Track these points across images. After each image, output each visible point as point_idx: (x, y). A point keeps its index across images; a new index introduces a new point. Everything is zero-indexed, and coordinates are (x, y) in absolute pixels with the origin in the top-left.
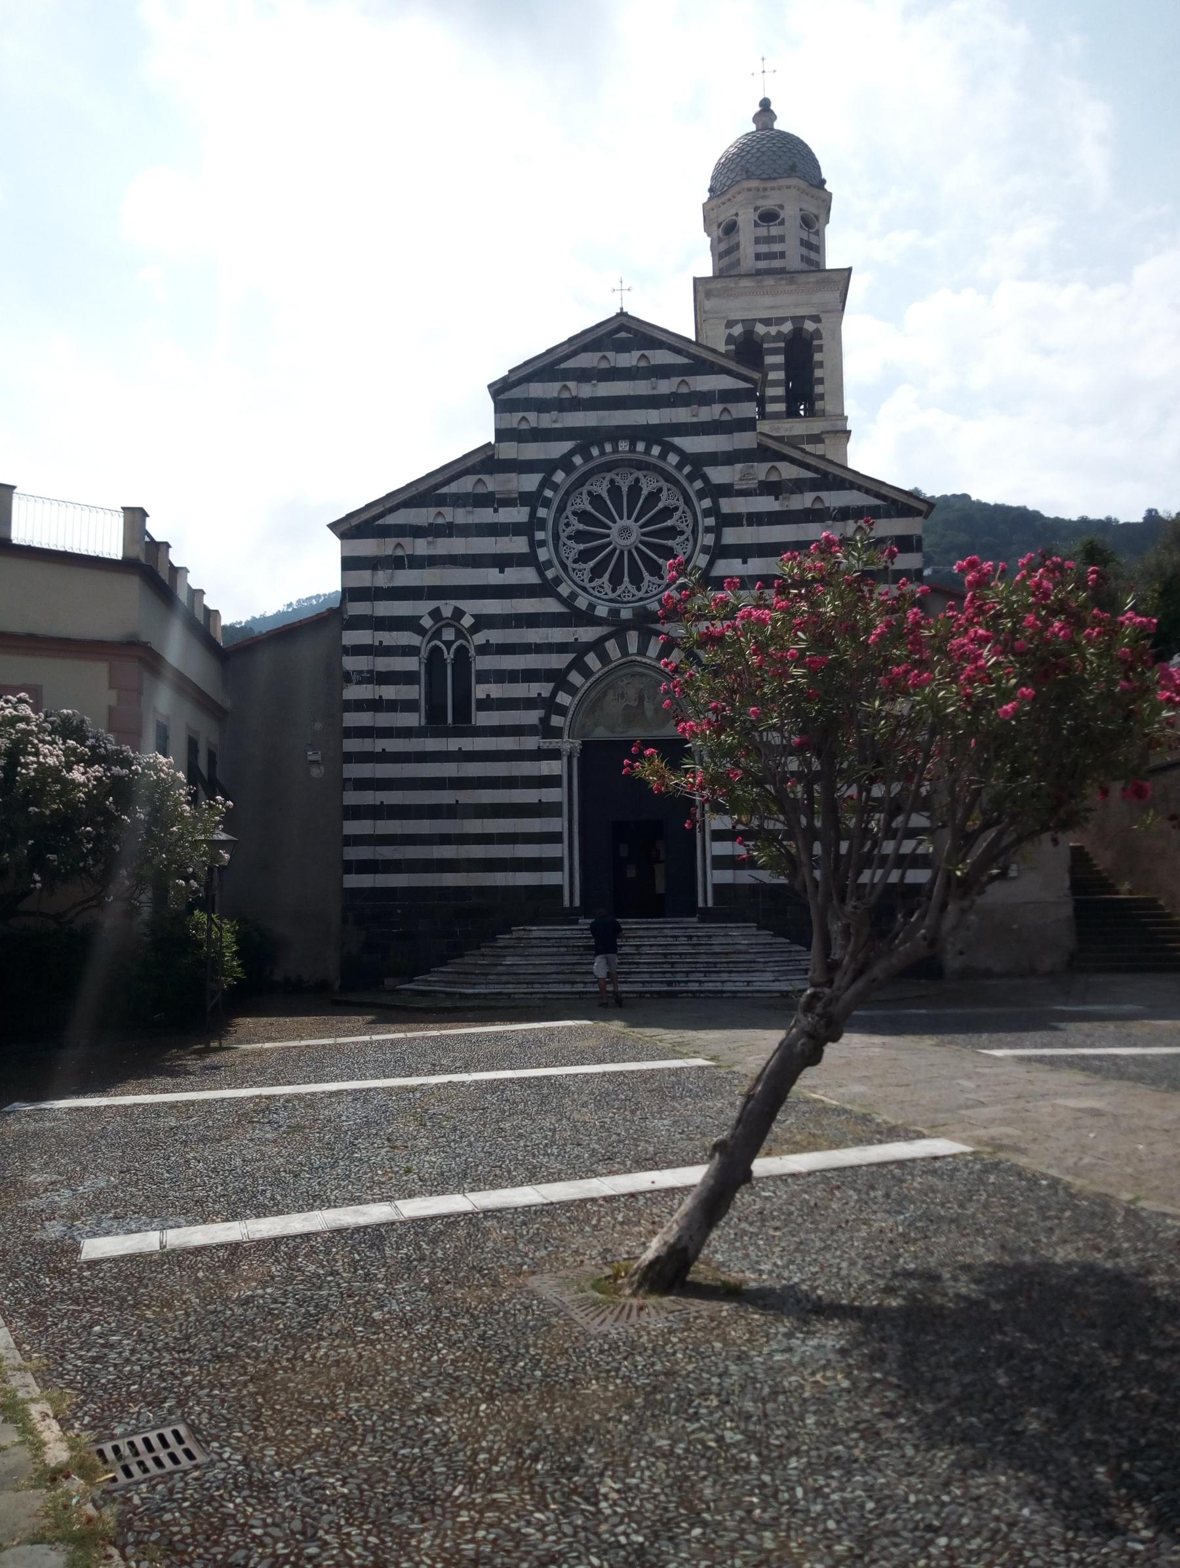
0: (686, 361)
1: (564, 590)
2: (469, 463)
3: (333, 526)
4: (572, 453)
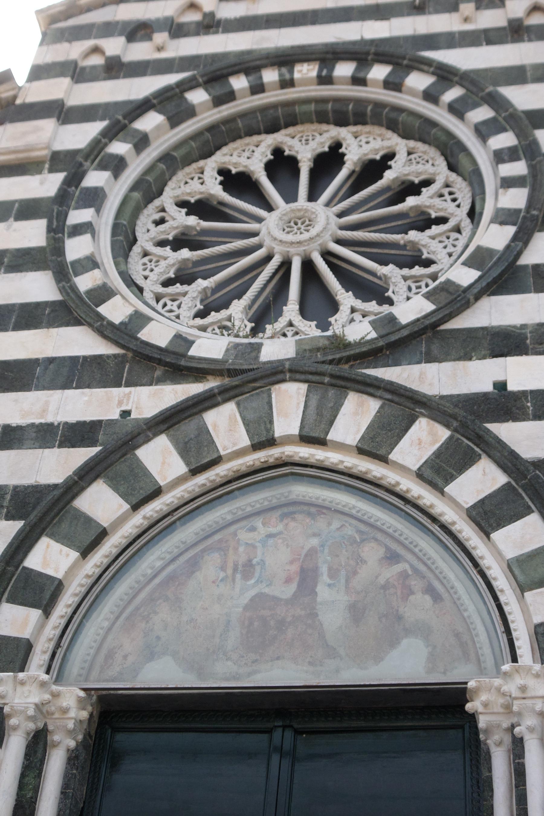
1: (115, 311)
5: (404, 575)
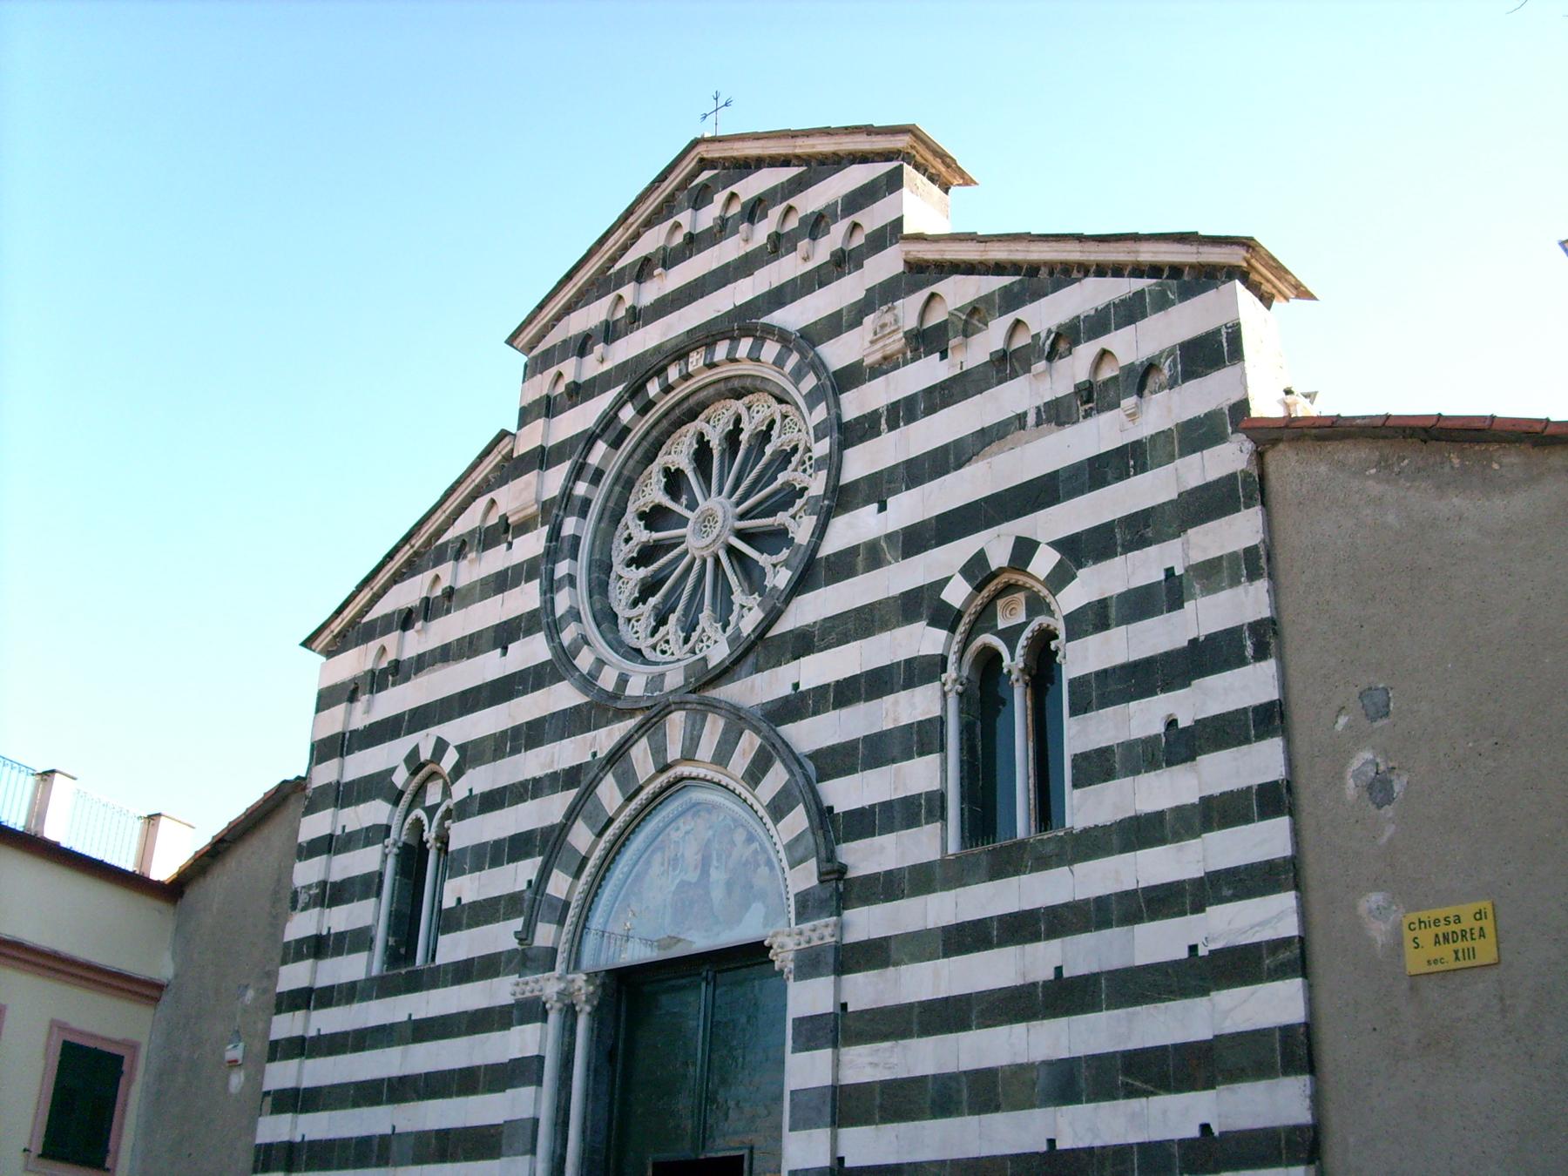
0: (792, 172)
2: (478, 477)
3: (308, 643)
4: (618, 404)
5: (756, 852)
